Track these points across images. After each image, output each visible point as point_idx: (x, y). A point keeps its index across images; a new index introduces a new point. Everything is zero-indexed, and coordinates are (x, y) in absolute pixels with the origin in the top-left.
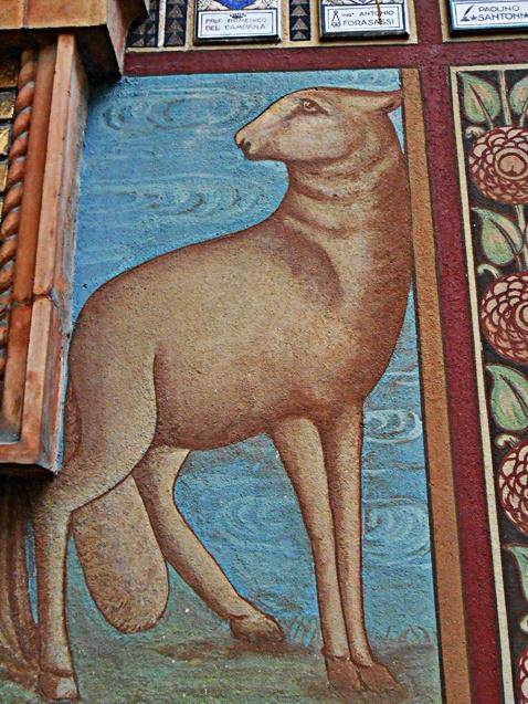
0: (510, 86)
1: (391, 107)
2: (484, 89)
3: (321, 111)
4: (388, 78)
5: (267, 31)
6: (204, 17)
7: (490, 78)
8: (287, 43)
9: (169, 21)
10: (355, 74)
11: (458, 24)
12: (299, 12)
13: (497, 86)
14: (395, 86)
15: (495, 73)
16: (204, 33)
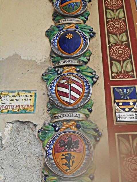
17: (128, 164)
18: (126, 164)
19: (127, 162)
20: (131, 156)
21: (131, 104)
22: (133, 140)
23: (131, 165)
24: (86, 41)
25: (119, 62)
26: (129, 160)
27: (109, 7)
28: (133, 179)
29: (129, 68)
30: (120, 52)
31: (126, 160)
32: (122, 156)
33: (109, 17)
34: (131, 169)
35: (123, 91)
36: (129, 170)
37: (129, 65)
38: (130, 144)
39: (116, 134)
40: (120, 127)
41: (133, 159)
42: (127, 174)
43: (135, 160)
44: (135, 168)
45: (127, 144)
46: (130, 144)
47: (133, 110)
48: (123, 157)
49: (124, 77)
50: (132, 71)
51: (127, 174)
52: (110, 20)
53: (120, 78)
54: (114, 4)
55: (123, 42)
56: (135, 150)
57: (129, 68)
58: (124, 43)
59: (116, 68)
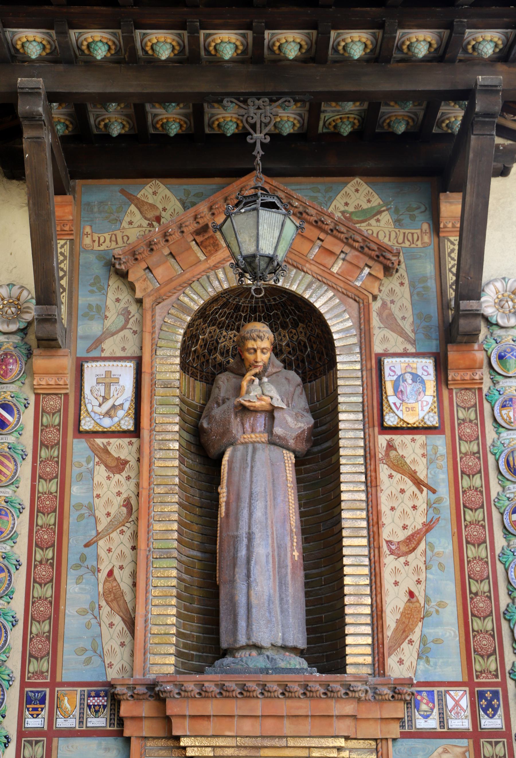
0: (496, 745)
1: (466, 751)
2: (489, 746)
3: (448, 752)
4: (464, 742)
5: (434, 727)
6: (418, 721)
7: (490, 743)
8: (439, 730)
9: (408, 721)
10: (457, 740)
11: (483, 727)
12: (442, 720)
13: (492, 746)
14: (466, 745)
15: (491, 742)
16: (418, 726)
21: (40, 709)
24: (6, 632)
25: (37, 659)
27: (38, 580)
29: (44, 669)
30: (40, 646)
33: (36, 595)
35: (35, 695)
37: (46, 664)
47: (40, 716)
49: (38, 679)
50: (47, 671)
52: (36, 600)
53: (35, 679)
54: (44, 575)
55: (44, 633)
57: (44, 669)
58: (45, 635)
59: (33, 666)
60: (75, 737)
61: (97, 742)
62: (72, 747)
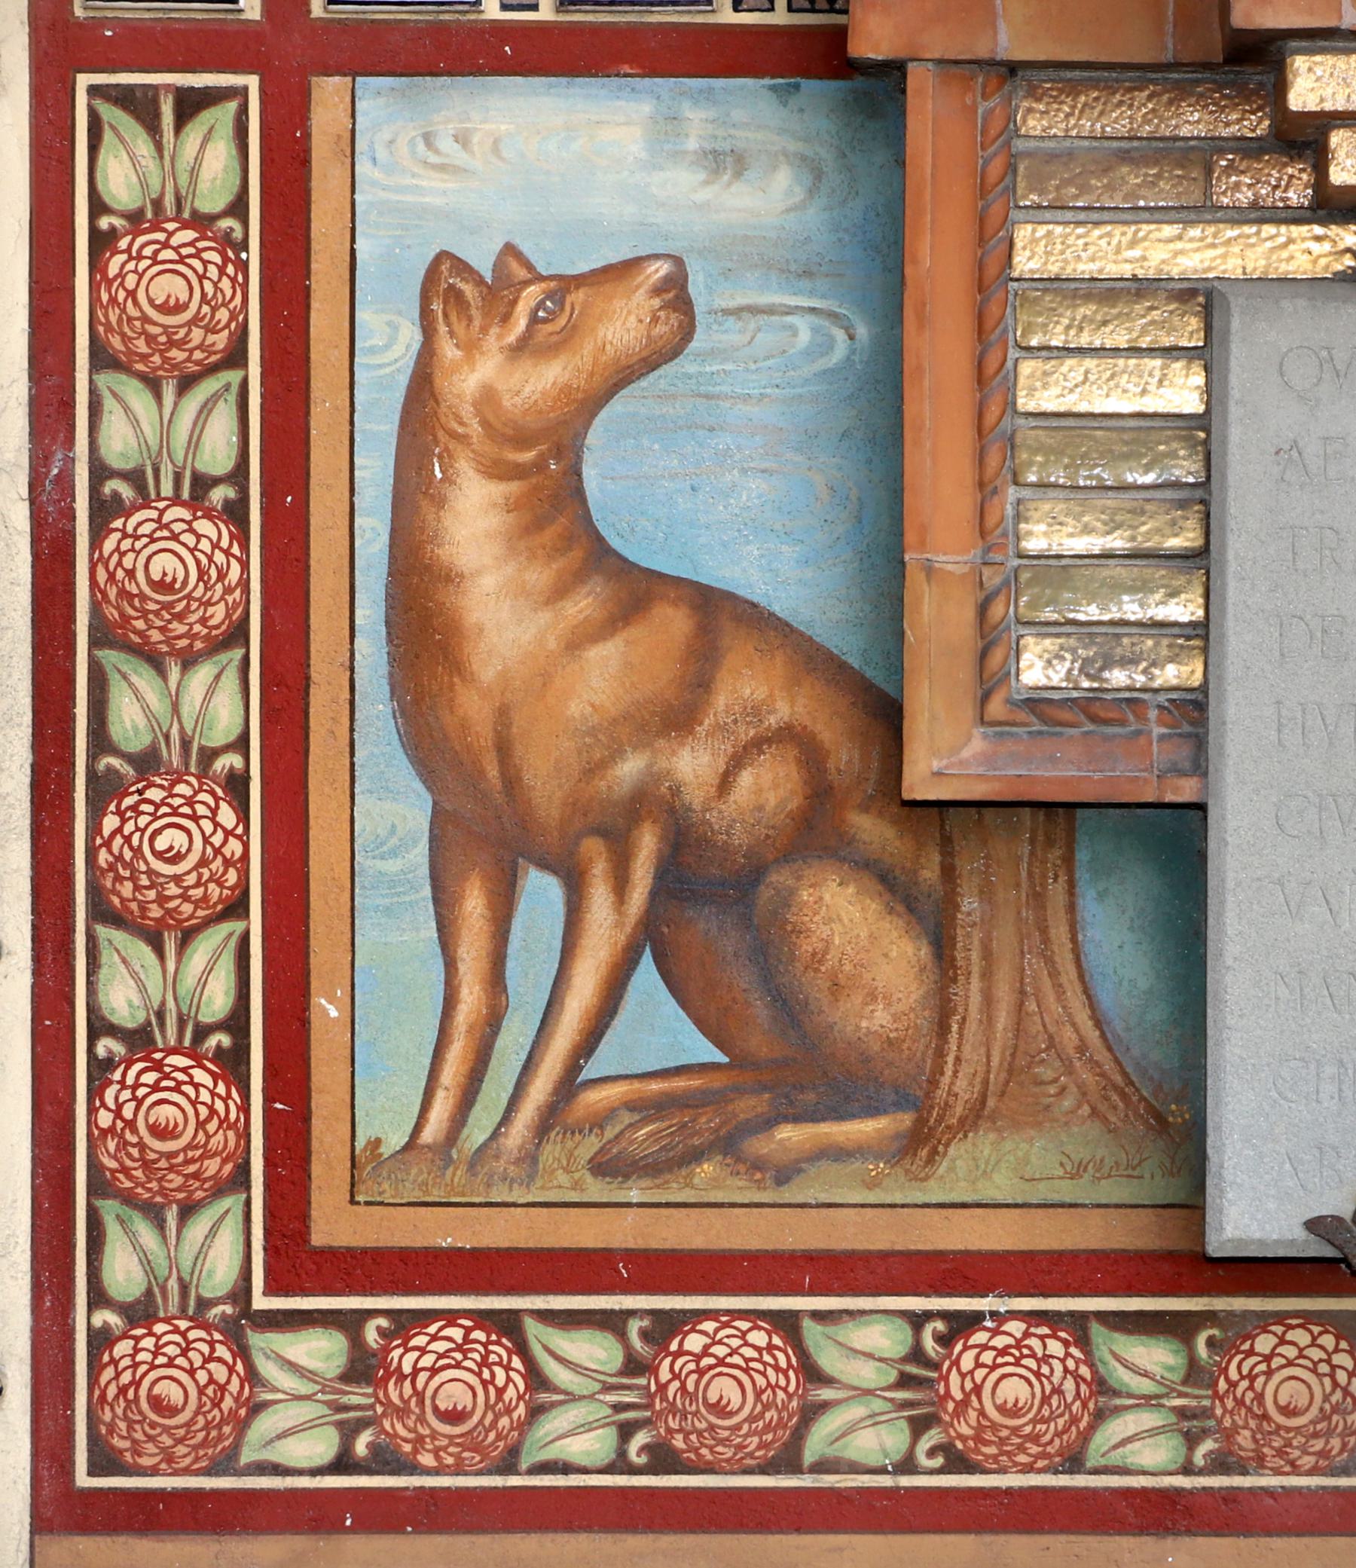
17: (135, 271)
18: (122, 275)
19: (130, 258)
20: (156, 227)
22: (182, 119)
23: (152, 279)
26: (143, 246)
28: (157, 359)
31: (128, 250)
32: (104, 223)
34: (151, 301)
36: (136, 303)
38: (159, 147)
39: (83, 81)
40: (109, 33)
41: (166, 245)
42: (126, 329)
43: (176, 249)
44: (172, 302)
45: (144, 146)
46: (159, 147)
48: (113, 229)
51: (126, 329)
56: (183, 192)
60: (477, 71)
61: (646, 108)
62: (462, 139)
